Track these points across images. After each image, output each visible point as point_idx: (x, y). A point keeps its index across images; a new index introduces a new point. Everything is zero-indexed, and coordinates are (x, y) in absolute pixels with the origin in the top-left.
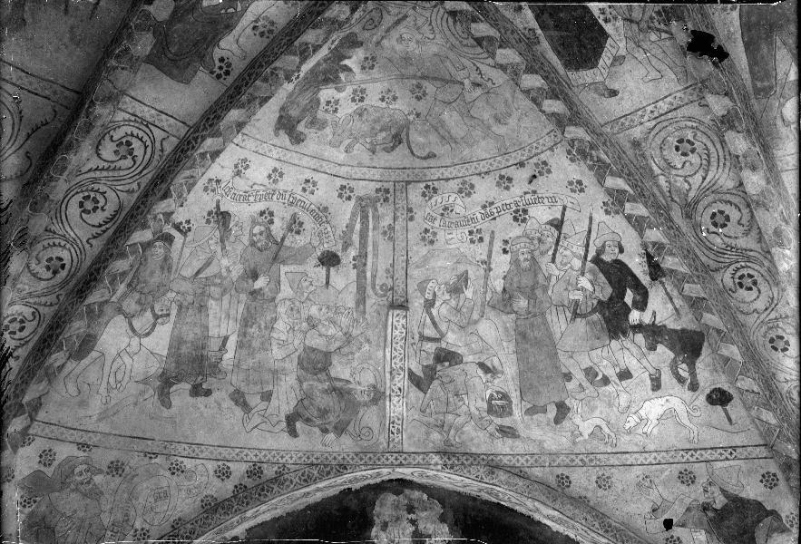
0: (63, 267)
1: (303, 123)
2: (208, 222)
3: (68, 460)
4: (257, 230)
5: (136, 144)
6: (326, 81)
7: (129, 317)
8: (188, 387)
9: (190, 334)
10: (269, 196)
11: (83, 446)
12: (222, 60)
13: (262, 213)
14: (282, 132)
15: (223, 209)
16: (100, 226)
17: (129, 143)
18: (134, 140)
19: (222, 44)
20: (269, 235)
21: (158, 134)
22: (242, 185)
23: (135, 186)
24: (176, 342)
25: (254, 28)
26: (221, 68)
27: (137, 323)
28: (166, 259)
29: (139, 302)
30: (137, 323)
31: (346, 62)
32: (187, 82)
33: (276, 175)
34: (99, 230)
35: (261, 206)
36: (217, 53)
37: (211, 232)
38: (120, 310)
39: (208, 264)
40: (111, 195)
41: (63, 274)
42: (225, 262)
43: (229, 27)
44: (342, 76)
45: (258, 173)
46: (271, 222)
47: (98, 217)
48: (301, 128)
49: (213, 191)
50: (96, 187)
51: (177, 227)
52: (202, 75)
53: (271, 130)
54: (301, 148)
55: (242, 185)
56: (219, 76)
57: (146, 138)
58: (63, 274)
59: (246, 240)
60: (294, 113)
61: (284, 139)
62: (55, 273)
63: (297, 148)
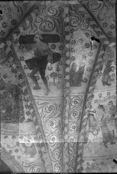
0: (75, 127)
1: (109, 81)
2: (99, 108)
3: (92, 163)
4: (110, 106)
5: (77, 101)
6: (109, 71)
7: (92, 132)
8: (110, 143)
9: (106, 132)
10: (109, 98)
11: (94, 160)
12: (85, 79)
13: (110, 102)
14: (105, 85)
15: (101, 105)
16: (78, 117)
17: (76, 101)
18: (77, 100)
19: (83, 76)
20: (113, 106)
21: (80, 97)
22: (102, 99)
23: (81, 108)
24: (104, 134)
25: (87, 71)
26: (85, 81)
27: (94, 133)
28: (94, 119)
29: (93, 129)
30: (94, 133)
31: (111, 66)
32: (81, 86)
33: (109, 94)
34: (78, 118)
35: (109, 101)
36: (83, 78)
37: (101, 111)
38: (90, 132)
39: (103, 116)
40: (77, 111)
41: (76, 128)
42: (106, 115)
43: (83, 73)
44: (112, 69)
45: (105, 95)
46: (112, 103)
47: (77, 116)
48: (109, 82)
49: (97, 102)
50: (74, 111)
51: (93, 112)
52: (83, 83)
53: (102, 86)
54: (111, 86)
55: (102, 99)
56: (86, 82)
57: (78, 99)
58: (76, 128)
59: (109, 109)
60: (106, 80)
61: (106, 86)
62: (74, 129)
63: (110, 87)
